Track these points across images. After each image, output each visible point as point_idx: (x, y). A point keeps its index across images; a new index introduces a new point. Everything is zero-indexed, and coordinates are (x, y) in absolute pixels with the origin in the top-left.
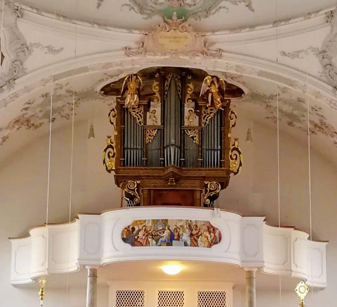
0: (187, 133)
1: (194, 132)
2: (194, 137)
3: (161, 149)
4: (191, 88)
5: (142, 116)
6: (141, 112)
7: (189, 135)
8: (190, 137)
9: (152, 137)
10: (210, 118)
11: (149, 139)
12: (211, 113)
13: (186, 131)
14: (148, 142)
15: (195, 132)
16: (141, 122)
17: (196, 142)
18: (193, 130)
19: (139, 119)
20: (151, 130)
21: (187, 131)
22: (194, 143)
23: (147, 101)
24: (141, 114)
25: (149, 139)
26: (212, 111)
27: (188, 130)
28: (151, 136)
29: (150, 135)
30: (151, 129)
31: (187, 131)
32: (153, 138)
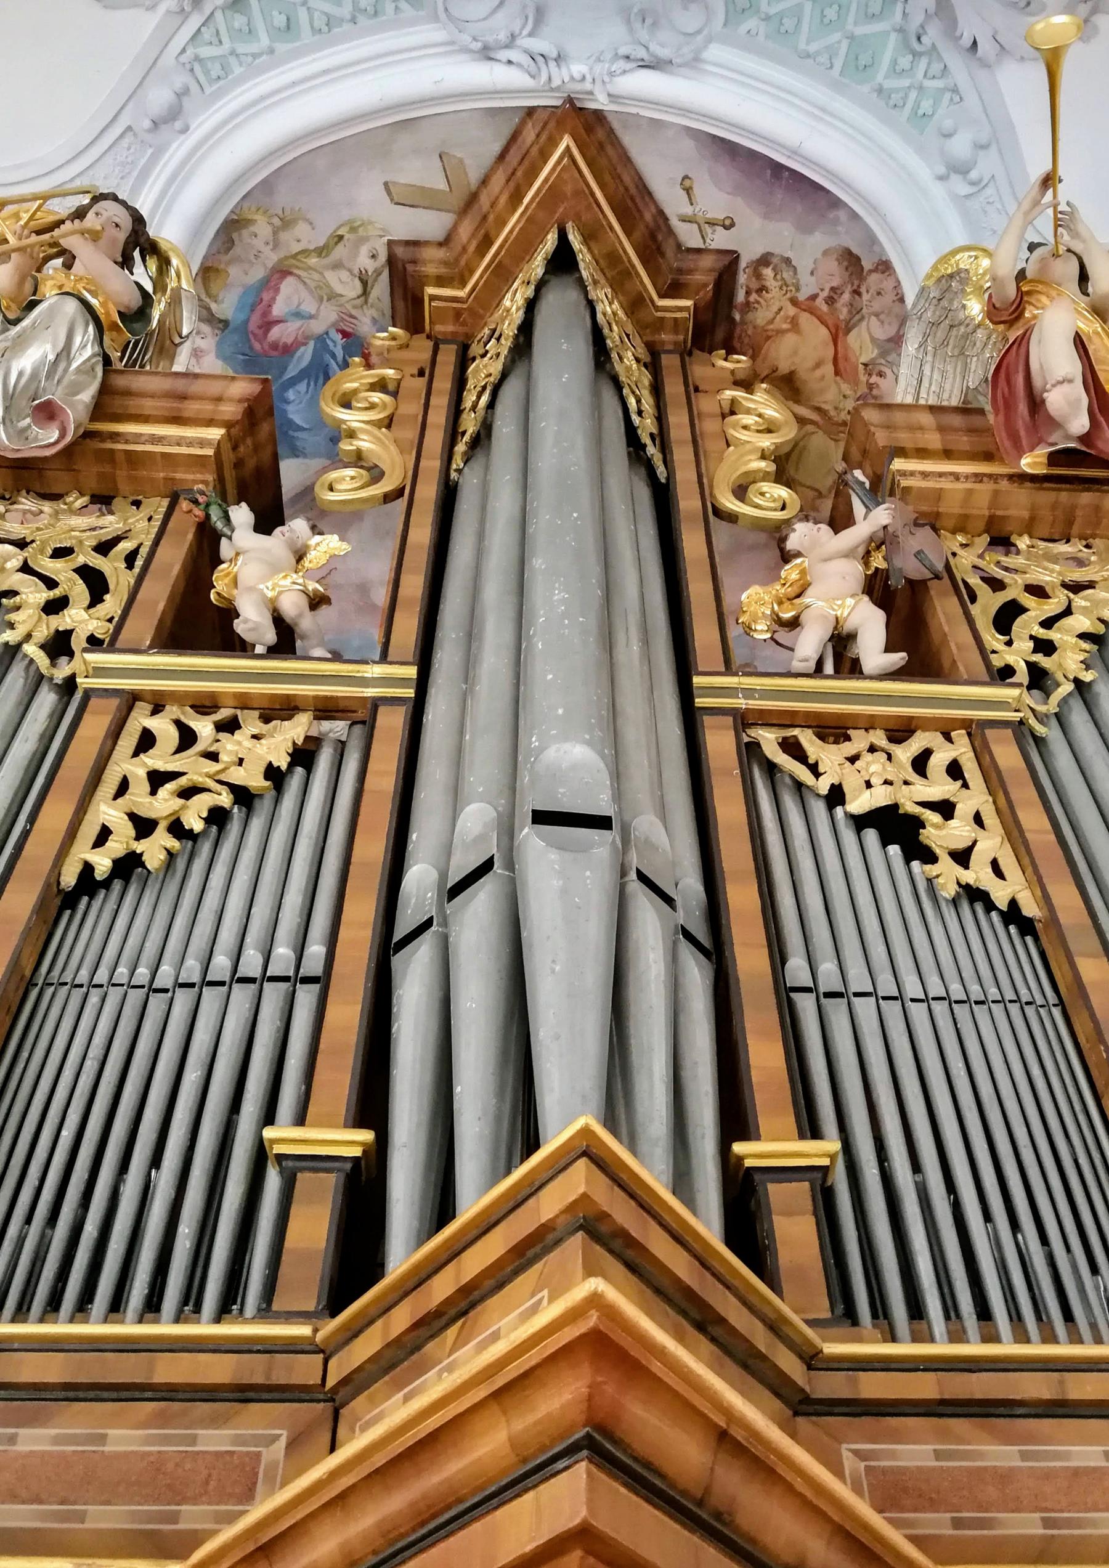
0: (804, 774)
1: (905, 753)
2: (918, 823)
3: (323, 981)
4: (760, 416)
5: (119, 578)
6: (126, 546)
7: (836, 796)
8: (860, 822)
9: (201, 804)
10: (1081, 622)
11: (144, 827)
12: (1076, 588)
13: (768, 739)
14: (103, 864)
15: (920, 764)
16: (78, 643)
17: (978, 875)
18: (879, 738)
19: (55, 607)
20: (204, 727)
21: (793, 748)
22: (949, 890)
23: (216, 433)
24: (111, 566)
25: (144, 827)
26: (1078, 575)
27: (807, 738)
28: (187, 793)
29: (174, 776)
30: (204, 705)
31: (793, 748)
32: (217, 817)
